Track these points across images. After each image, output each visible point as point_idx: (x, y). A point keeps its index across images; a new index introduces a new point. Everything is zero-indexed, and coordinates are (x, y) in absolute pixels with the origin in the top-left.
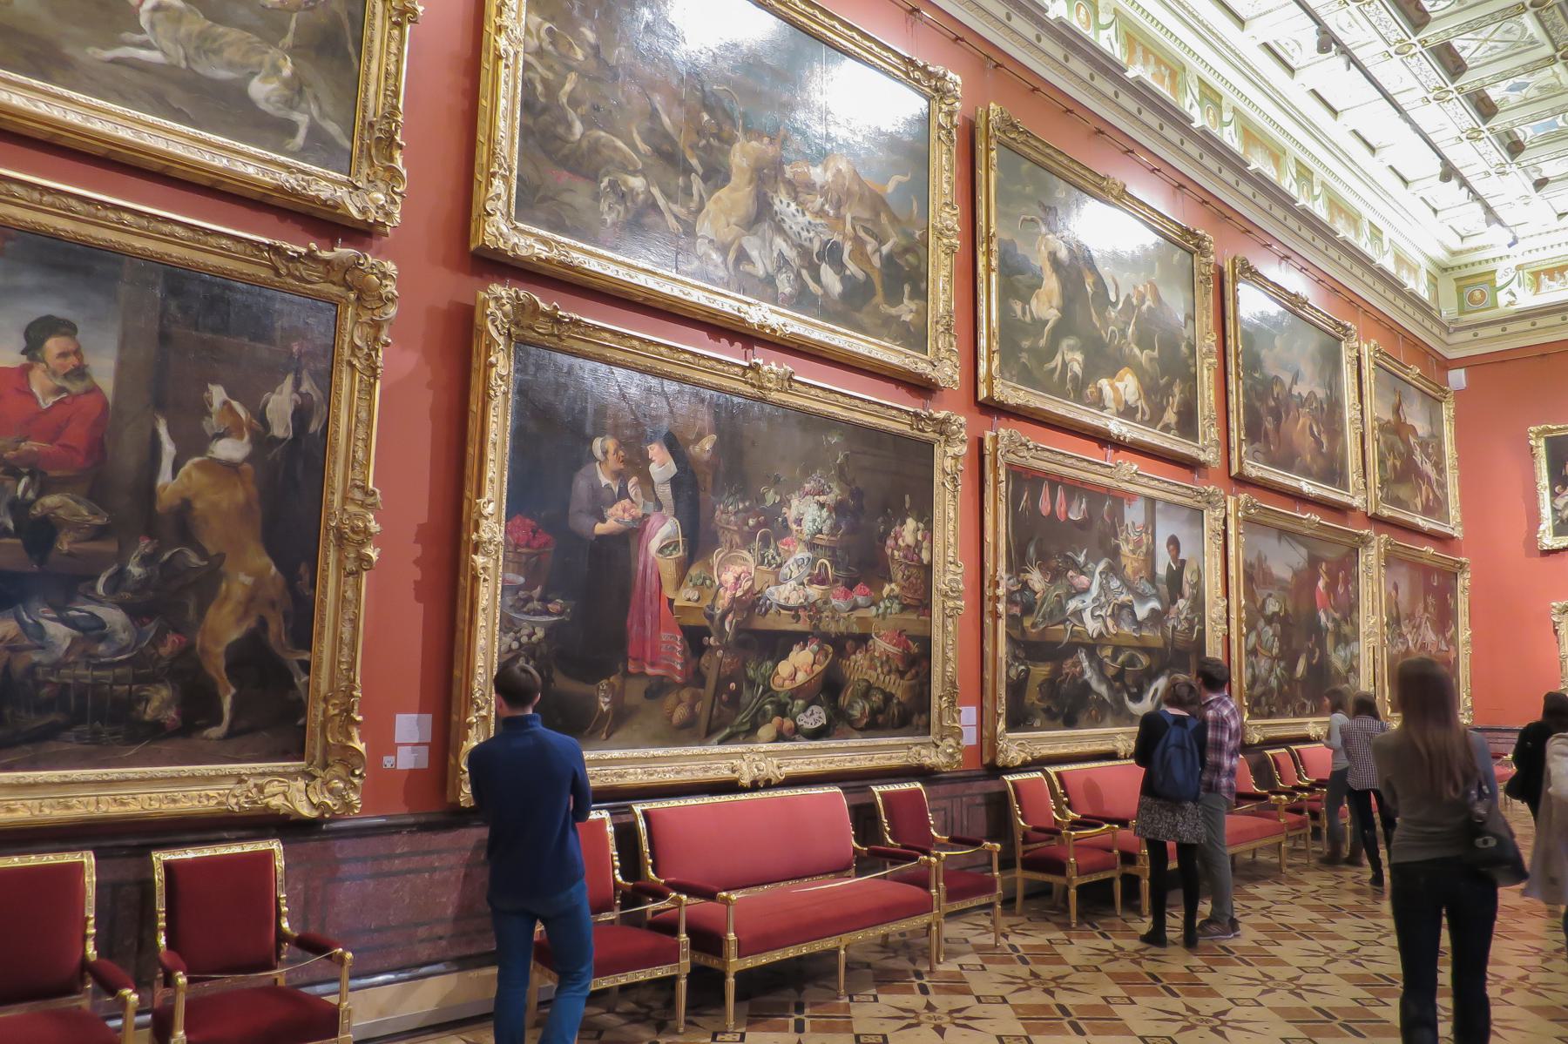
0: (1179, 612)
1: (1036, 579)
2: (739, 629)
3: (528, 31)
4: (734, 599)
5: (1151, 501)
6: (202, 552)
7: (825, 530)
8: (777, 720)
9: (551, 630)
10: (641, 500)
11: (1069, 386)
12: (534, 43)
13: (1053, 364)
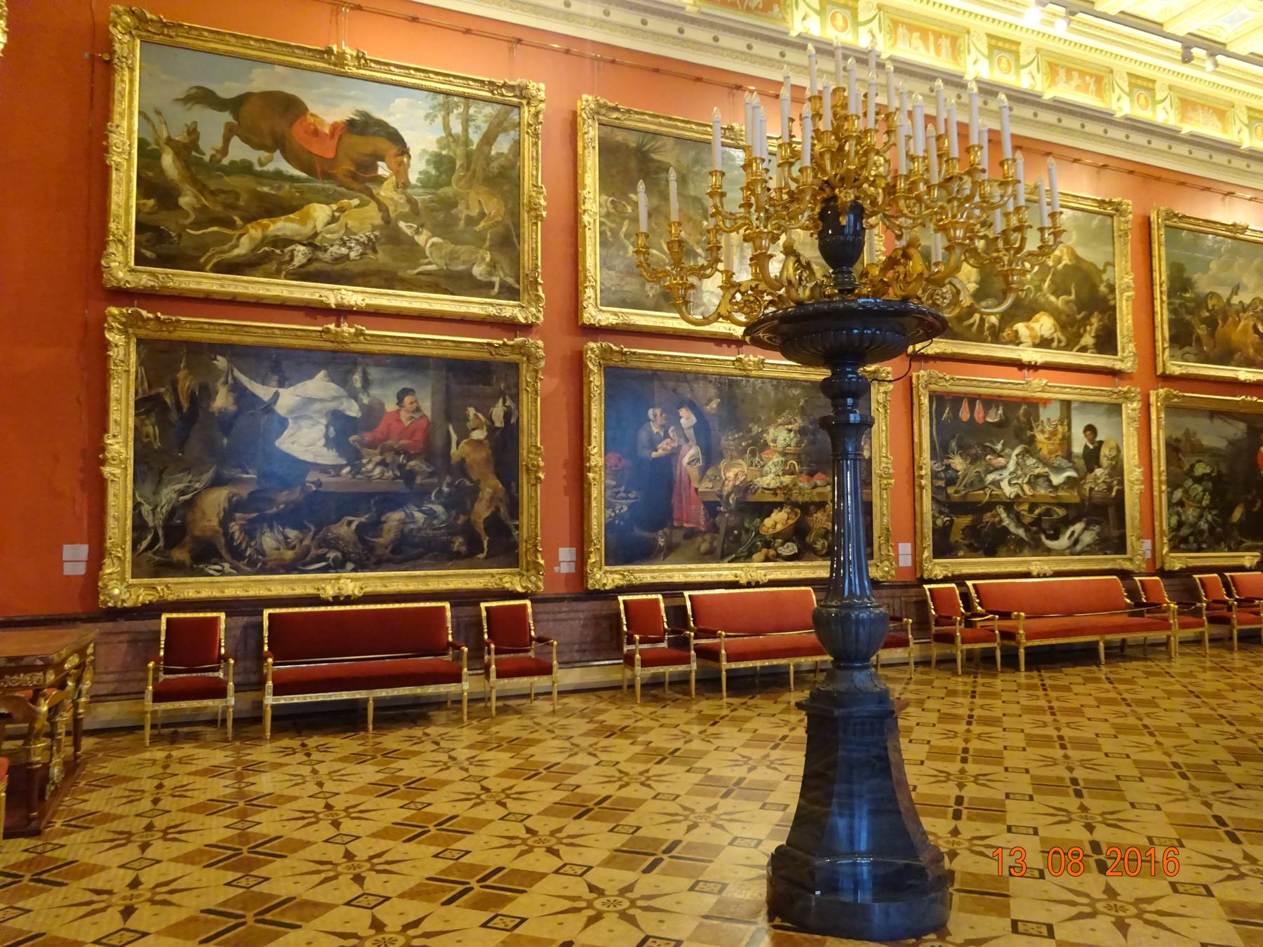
0: (1097, 478)
1: (958, 463)
2: (737, 502)
3: (600, 205)
4: (735, 486)
5: (1066, 405)
6: (471, 480)
7: (793, 444)
8: (764, 550)
9: (631, 506)
10: (676, 438)
11: (987, 333)
12: (604, 210)
13: (971, 321)
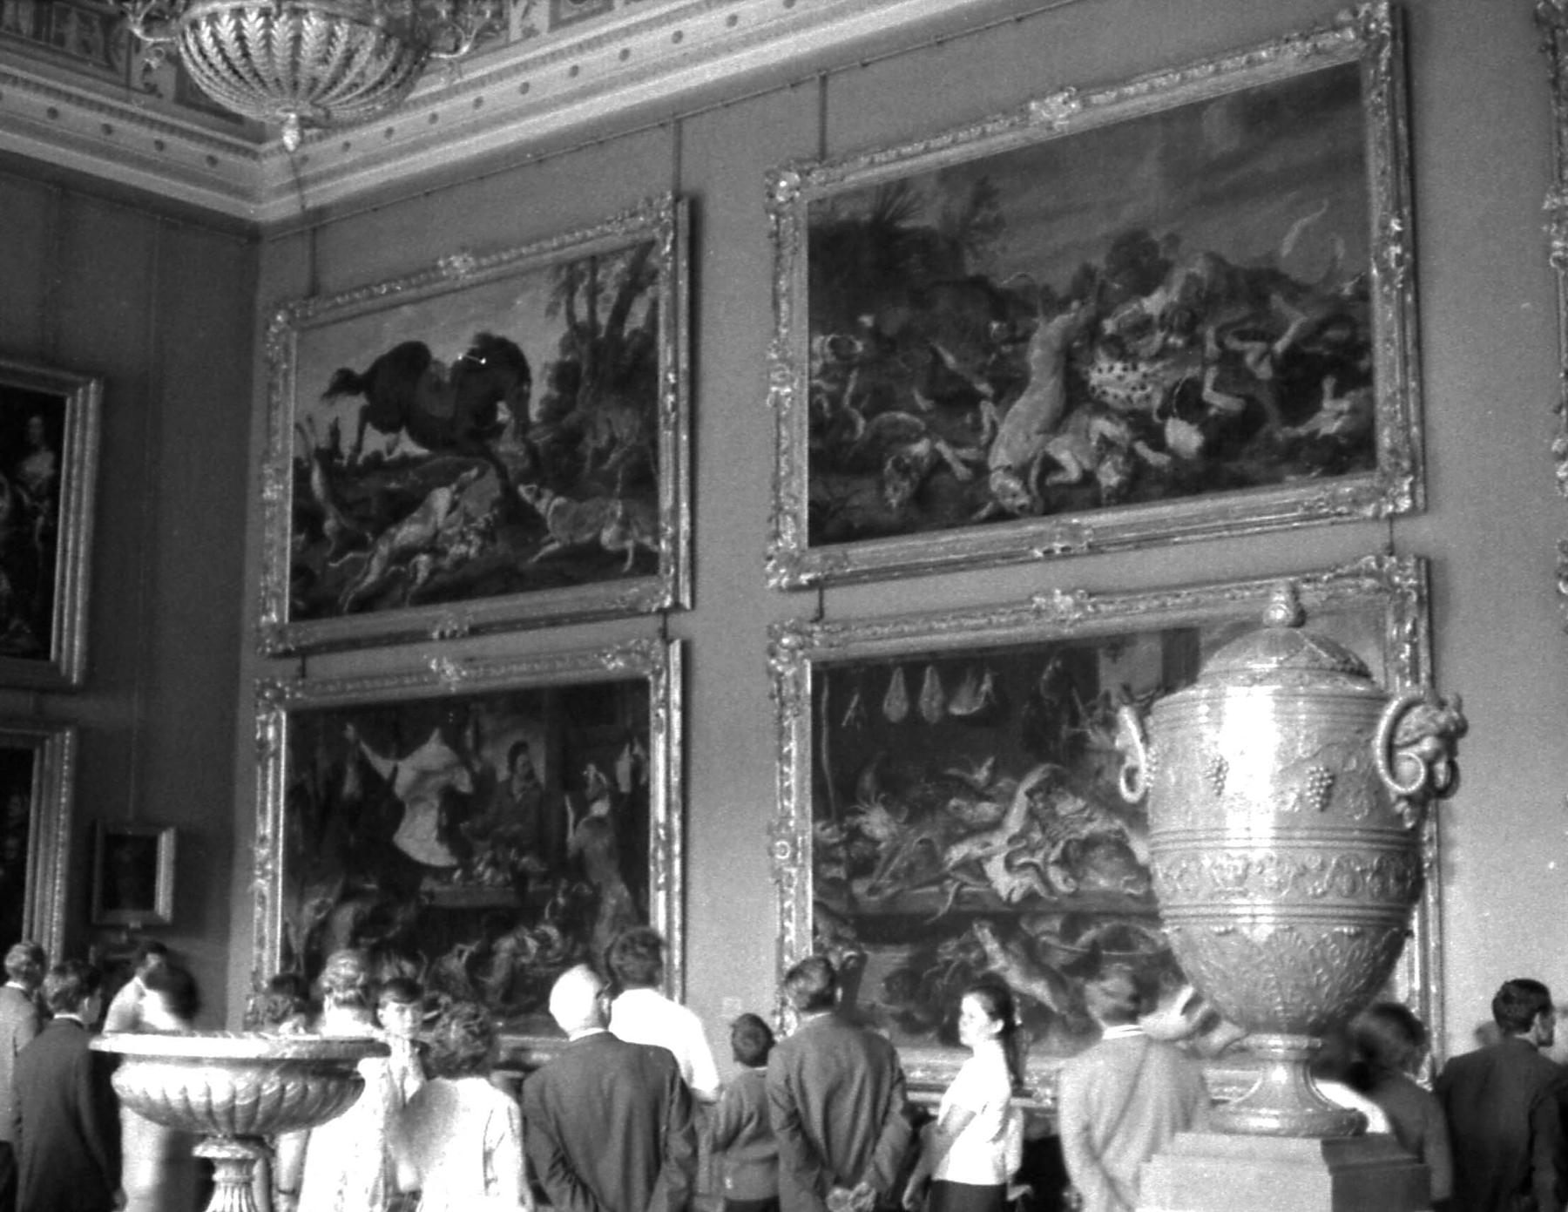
1: (877, 823)
